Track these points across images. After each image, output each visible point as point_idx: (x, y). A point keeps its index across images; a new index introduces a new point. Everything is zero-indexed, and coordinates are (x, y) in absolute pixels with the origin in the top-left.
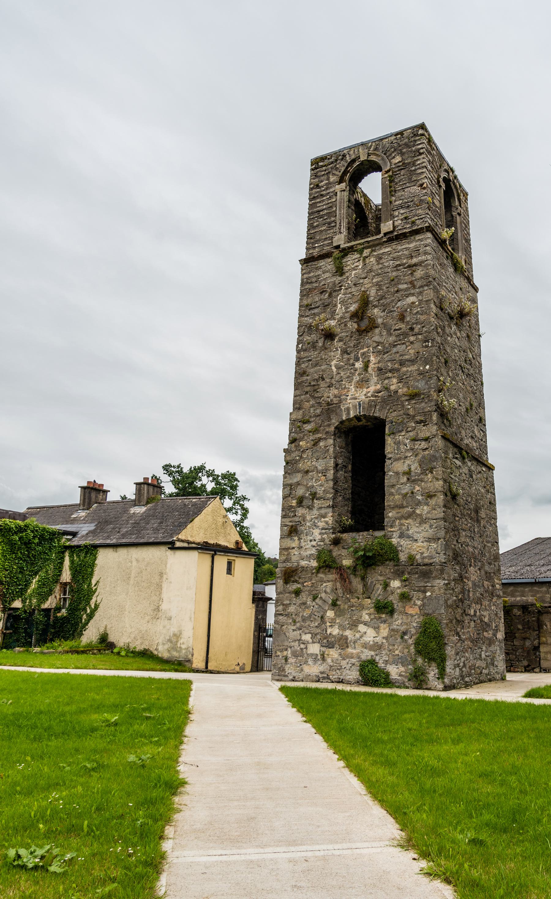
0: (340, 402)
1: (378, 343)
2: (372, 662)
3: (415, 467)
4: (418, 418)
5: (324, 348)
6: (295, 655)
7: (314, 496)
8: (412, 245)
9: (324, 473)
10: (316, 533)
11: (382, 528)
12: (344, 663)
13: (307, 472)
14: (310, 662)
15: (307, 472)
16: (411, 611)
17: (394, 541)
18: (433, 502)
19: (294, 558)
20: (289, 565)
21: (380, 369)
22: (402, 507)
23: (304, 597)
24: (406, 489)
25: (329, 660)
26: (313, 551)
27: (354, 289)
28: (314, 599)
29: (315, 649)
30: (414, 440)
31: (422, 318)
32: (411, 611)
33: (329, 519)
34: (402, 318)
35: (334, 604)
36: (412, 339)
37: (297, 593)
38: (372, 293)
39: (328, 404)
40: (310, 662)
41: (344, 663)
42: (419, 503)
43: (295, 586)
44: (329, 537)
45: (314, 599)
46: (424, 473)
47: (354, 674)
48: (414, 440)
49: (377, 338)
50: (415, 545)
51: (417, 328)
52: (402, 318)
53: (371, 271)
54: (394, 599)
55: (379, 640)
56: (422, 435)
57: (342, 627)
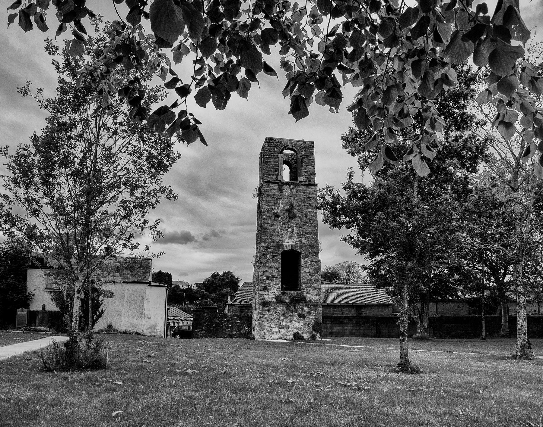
0: (282, 243)
1: (297, 224)
2: (298, 333)
3: (312, 271)
4: (313, 254)
5: (275, 220)
6: (268, 331)
7: (273, 276)
8: (310, 189)
9: (278, 268)
10: (275, 290)
11: (300, 290)
12: (287, 334)
13: (270, 267)
14: (274, 333)
15: (270, 267)
16: (311, 317)
17: (305, 294)
18: (318, 283)
19: (266, 298)
20: (264, 300)
21: (298, 233)
22: (307, 283)
23: (271, 312)
24: (309, 278)
25: (282, 333)
26: (274, 296)
27: (287, 200)
28: (276, 312)
29: (276, 329)
30: (312, 261)
31: (314, 218)
32: (311, 317)
33: (280, 285)
34: (306, 216)
35: (283, 315)
36: (310, 225)
37: (269, 311)
38: (295, 203)
39: (277, 242)
40: (274, 333)
41: (287, 334)
42: (313, 283)
43: (268, 308)
44: (280, 292)
45: (276, 312)
46: (315, 273)
47: (291, 337)
48: (312, 261)
49: (296, 221)
50: (312, 296)
51: (312, 221)
52: (306, 216)
53: (294, 194)
54: (305, 313)
55: (300, 326)
56: (314, 260)
57: (286, 322)
